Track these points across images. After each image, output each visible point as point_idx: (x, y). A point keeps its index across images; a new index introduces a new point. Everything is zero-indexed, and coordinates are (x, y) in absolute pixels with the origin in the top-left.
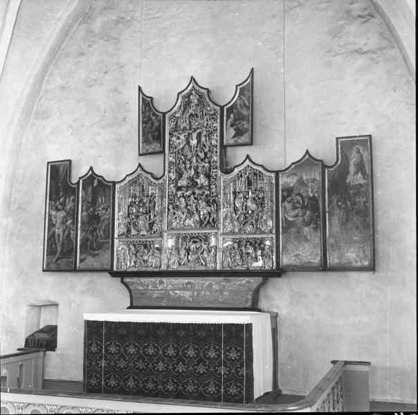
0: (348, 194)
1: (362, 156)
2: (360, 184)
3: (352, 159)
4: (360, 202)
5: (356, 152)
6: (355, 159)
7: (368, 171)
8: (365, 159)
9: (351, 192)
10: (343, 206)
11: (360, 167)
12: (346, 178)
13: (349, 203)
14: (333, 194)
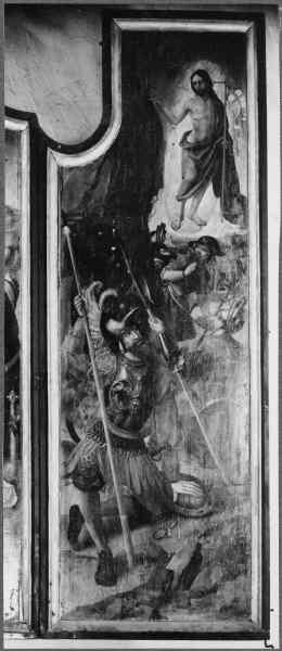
0: (158, 285)
1: (219, 109)
2: (212, 245)
3: (175, 122)
4: (206, 326)
5: (199, 93)
6: (187, 124)
7: (248, 187)
8: (233, 128)
9: (168, 274)
10: (131, 338)
11: (213, 162)
12: (149, 208)
13: (157, 326)
14: (85, 284)
